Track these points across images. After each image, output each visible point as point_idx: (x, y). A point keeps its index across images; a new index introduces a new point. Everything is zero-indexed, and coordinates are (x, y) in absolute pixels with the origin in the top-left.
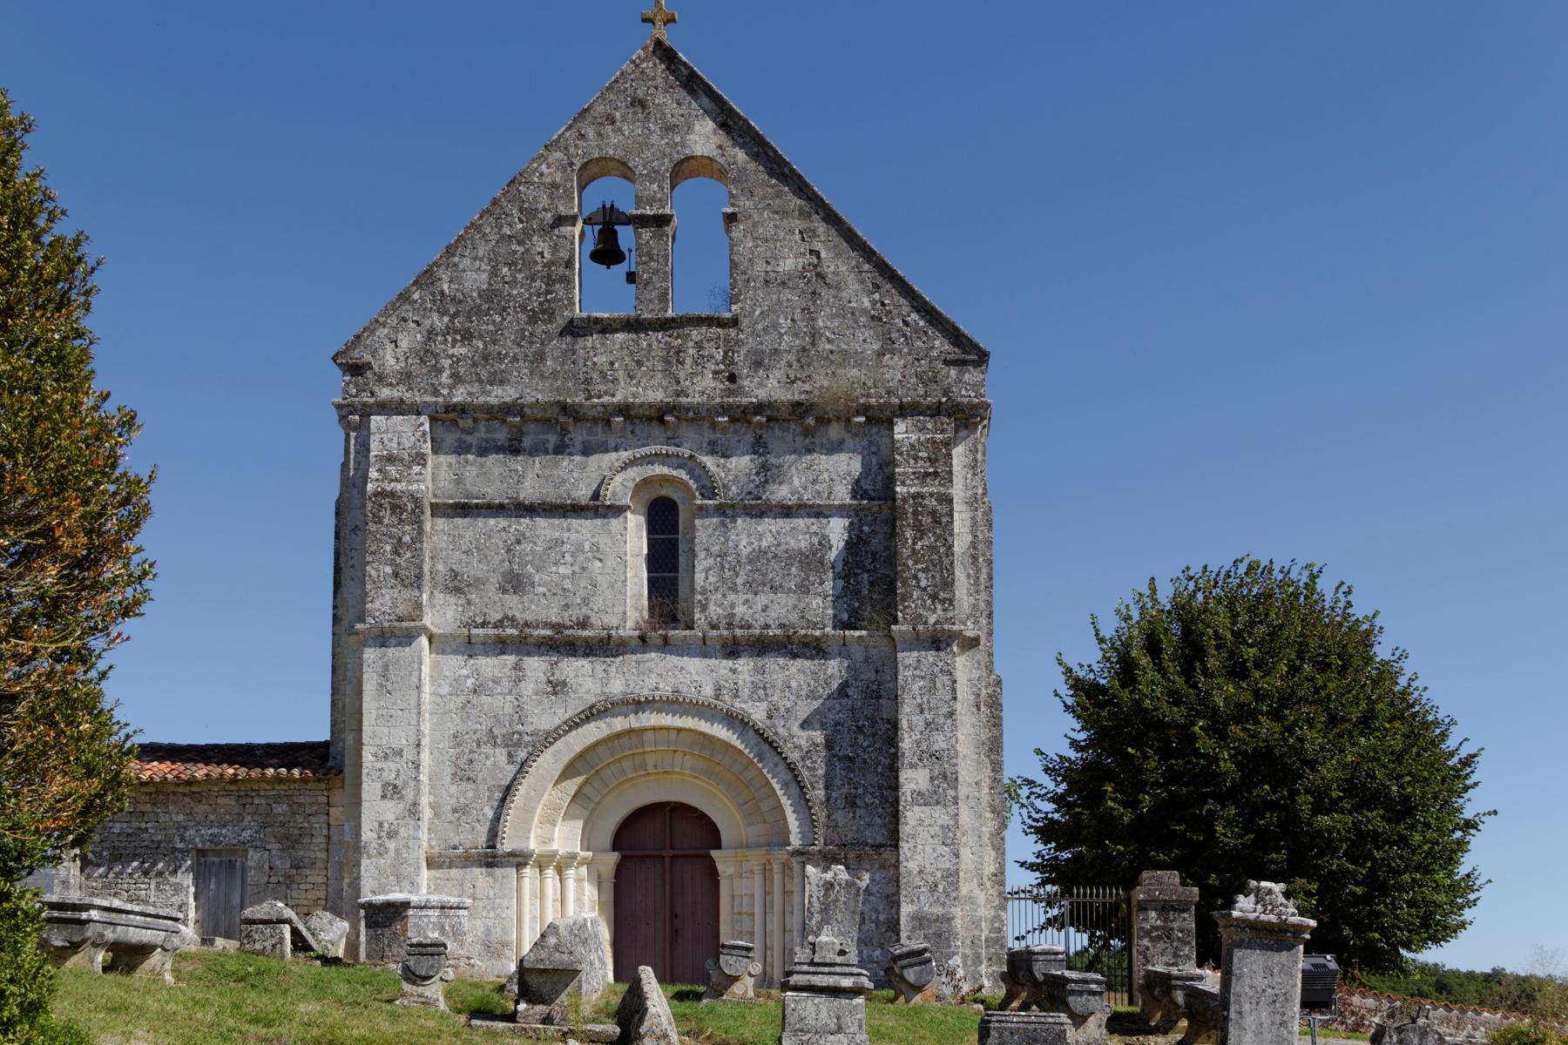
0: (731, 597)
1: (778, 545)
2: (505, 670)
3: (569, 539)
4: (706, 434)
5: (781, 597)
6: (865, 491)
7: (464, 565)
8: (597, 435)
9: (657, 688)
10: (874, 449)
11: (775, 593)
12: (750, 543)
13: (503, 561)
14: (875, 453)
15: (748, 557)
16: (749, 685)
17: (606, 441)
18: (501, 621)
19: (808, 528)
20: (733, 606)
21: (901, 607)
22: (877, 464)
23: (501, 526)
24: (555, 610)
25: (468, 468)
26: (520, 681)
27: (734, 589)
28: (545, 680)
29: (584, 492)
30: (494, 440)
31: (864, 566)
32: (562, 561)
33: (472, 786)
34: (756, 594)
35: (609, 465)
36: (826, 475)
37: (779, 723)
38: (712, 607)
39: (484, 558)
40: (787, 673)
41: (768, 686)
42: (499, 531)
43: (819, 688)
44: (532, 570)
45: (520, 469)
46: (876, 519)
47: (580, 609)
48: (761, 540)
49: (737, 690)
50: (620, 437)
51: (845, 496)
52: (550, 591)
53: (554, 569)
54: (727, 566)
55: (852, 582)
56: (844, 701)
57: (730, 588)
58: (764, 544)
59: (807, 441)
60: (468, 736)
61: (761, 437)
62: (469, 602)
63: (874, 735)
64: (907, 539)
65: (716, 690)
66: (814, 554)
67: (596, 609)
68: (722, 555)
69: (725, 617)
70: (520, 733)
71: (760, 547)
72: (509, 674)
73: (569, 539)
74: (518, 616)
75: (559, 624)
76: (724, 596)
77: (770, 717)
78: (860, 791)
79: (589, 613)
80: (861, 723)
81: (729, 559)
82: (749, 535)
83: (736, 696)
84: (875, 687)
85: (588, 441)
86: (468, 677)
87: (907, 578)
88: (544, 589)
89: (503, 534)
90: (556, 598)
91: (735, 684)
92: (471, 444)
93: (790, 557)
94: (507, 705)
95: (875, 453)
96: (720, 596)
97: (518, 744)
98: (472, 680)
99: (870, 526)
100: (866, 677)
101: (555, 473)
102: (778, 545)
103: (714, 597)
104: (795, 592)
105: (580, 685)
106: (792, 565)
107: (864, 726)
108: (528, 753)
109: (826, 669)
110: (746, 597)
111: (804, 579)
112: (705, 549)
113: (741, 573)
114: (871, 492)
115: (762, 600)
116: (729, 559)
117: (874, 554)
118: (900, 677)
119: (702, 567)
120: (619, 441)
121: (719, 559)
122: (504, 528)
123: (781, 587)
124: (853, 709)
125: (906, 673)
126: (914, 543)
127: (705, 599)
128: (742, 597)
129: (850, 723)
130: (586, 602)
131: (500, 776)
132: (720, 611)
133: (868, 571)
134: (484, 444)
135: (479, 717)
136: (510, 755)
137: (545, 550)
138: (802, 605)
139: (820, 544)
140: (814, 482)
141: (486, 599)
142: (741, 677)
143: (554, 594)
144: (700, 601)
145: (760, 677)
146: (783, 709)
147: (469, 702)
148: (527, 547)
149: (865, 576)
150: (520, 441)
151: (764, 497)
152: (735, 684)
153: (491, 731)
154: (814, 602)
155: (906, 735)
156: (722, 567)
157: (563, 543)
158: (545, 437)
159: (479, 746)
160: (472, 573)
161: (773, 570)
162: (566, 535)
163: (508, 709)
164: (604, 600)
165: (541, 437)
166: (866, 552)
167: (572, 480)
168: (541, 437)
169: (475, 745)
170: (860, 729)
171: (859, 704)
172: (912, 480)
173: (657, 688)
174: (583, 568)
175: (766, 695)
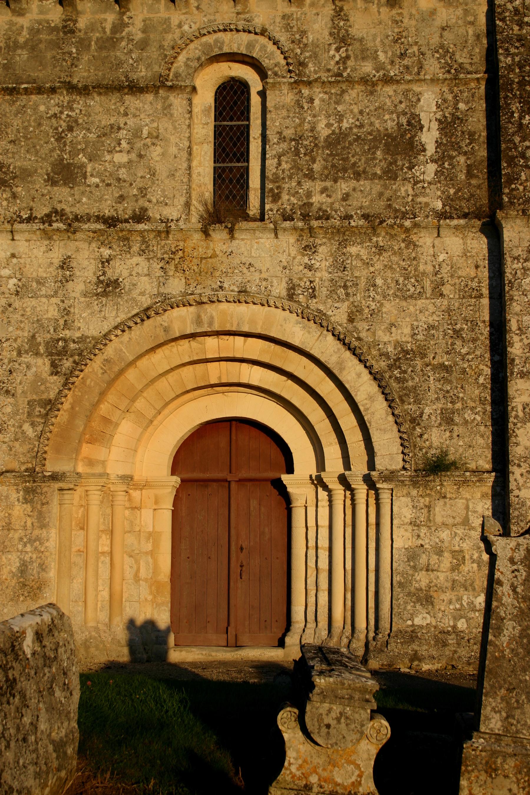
0: (307, 185)
1: (361, 126)
2: (51, 269)
3: (126, 124)
4: (279, 7)
5: (364, 184)
6: (461, 65)
7: (10, 155)
8: (159, 12)
9: (221, 287)
10: (470, 18)
11: (358, 181)
12: (329, 125)
13: (52, 150)
14: (472, 23)
15: (326, 140)
16: (327, 284)
17: (169, 18)
18: (48, 216)
19: (396, 106)
20: (309, 194)
21: (507, 191)
22: (474, 35)
23: (51, 112)
24: (109, 202)
25: (19, 51)
26: (67, 281)
27: (310, 176)
28: (95, 280)
29: (143, 74)
30: (48, 22)
31: (460, 147)
32: (118, 149)
33: (11, 400)
34: (335, 181)
35: (172, 43)
36: (415, 48)
37: (363, 326)
38: (285, 197)
39: (32, 149)
40: (372, 269)
41: (349, 284)
42: (50, 118)
43: (410, 286)
44: (84, 160)
45: (74, 50)
46: (473, 96)
47: (137, 201)
48: (340, 121)
49: (314, 289)
50: (184, 14)
51: (438, 70)
52: (104, 181)
53: (108, 157)
54: (302, 151)
55: (446, 165)
56: (438, 302)
57: (306, 176)
58: (345, 125)
59: (394, 12)
60: (8, 343)
61: (341, 9)
62: (14, 196)
63: (474, 340)
64: (513, 113)
65: (289, 290)
66: (402, 136)
67: (154, 200)
68: (298, 139)
69: (301, 207)
70: (65, 340)
71: (340, 128)
72: (54, 274)
73: (126, 124)
74: (68, 210)
75: (113, 218)
76: (299, 183)
77: (351, 320)
78: (459, 405)
79: (147, 204)
80: (458, 327)
81: (305, 143)
82: (328, 116)
83: (313, 296)
84: (475, 284)
85: (150, 19)
86: (10, 277)
87: (513, 158)
88: (97, 180)
89: (54, 120)
90: (110, 189)
91: (311, 282)
92: (22, 27)
93: (375, 139)
94: (51, 309)
95: (472, 23)
96: (294, 184)
97: (64, 352)
98: (14, 281)
99: (467, 103)
100: (464, 274)
101: (112, 54)
102: (361, 126)
103: (286, 186)
104: (380, 178)
105: (134, 285)
106: (377, 148)
107: (463, 329)
108: (74, 362)
109: (417, 266)
110: (324, 184)
111: (391, 164)
112: (278, 133)
113: (319, 158)
114: (468, 66)
115: (344, 186)
116: (305, 143)
117: (471, 134)
118: (508, 270)
119: (274, 152)
120: (183, 17)
121: (293, 143)
122: (55, 114)
123: (364, 172)
124: (449, 311)
125: (515, 266)
126: (521, 118)
127: (278, 187)
128: (319, 185)
129: (446, 327)
130: (143, 192)
131: (43, 388)
132: (294, 200)
133: (465, 153)
134: (36, 26)
135: (21, 322)
136: (53, 365)
137: (99, 137)
138: (388, 193)
139: (409, 123)
140: (403, 56)
141: (33, 192)
142: (318, 274)
143: (108, 185)
144: (272, 190)
145: (340, 274)
146: (366, 311)
147: (10, 305)
148: (79, 134)
149: (462, 159)
150: (75, 21)
151: (345, 74)
152: (311, 282)
153: (33, 337)
154: (403, 189)
155: (516, 338)
156: (297, 153)
157: (119, 128)
158: (103, 16)
159: (19, 354)
160: (18, 164)
161: (356, 154)
162: (122, 121)
163: (53, 312)
164: (163, 191)
165: (97, 17)
166: (463, 132)
167: (131, 61)
168: (97, 17)
169: (15, 353)
170: (457, 333)
171: (457, 304)
172: (517, 48)
173: (221, 287)
174: (140, 156)
175: (347, 295)
